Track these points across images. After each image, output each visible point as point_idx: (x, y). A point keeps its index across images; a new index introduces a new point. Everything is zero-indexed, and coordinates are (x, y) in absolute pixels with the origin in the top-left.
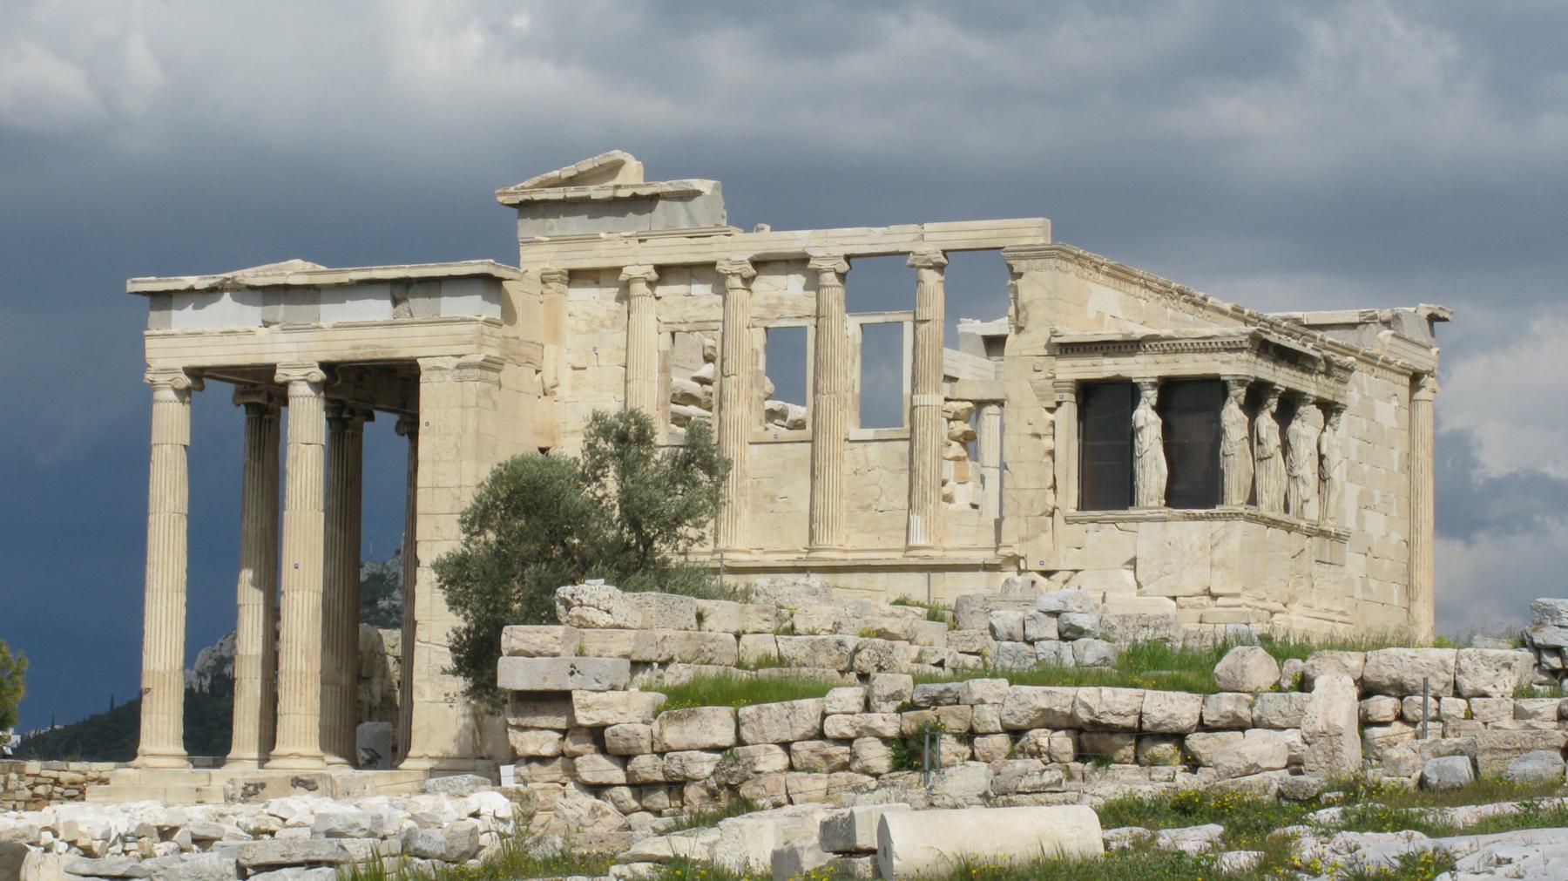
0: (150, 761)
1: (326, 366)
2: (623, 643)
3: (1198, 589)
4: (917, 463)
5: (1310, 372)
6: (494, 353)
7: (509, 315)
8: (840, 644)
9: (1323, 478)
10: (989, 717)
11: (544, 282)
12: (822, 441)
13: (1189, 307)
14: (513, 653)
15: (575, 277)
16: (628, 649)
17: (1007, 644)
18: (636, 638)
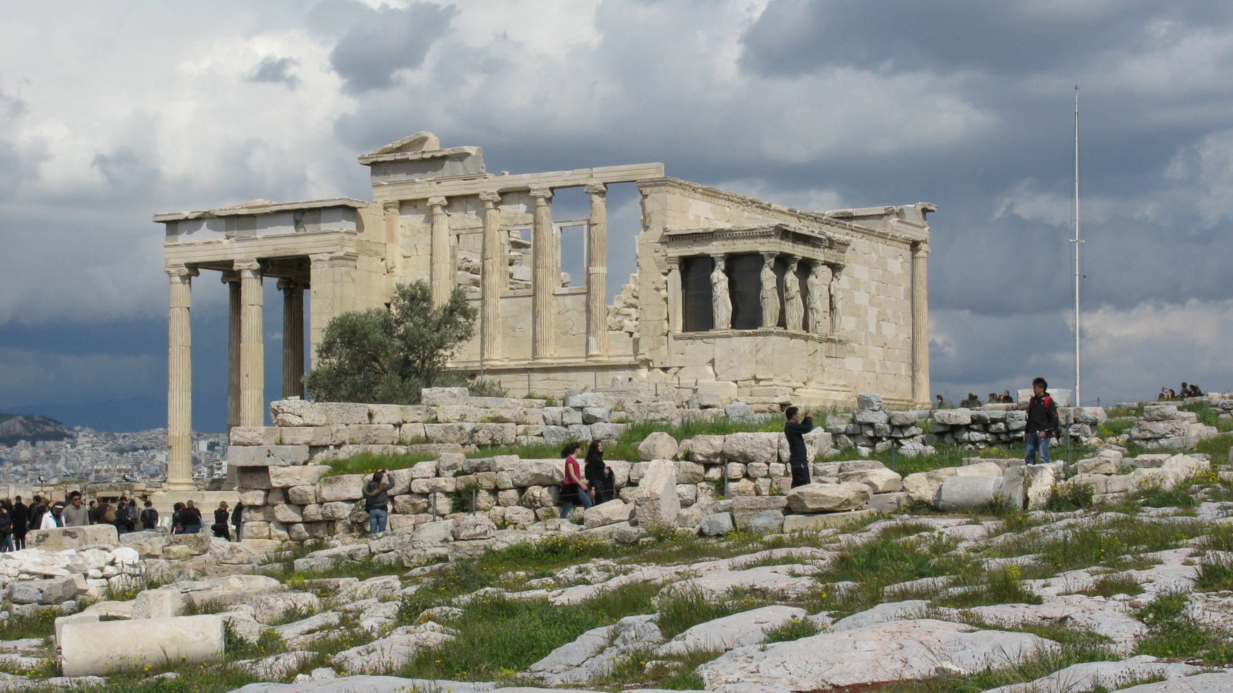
0: (172, 487)
1: (260, 260)
2: (307, 435)
3: (749, 376)
4: (592, 307)
5: (819, 247)
6: (352, 250)
7: (360, 227)
8: (461, 428)
9: (832, 308)
10: (506, 479)
11: (385, 208)
12: (540, 296)
13: (759, 210)
14: (236, 444)
15: (403, 205)
16: (309, 439)
17: (553, 427)
18: (315, 432)
